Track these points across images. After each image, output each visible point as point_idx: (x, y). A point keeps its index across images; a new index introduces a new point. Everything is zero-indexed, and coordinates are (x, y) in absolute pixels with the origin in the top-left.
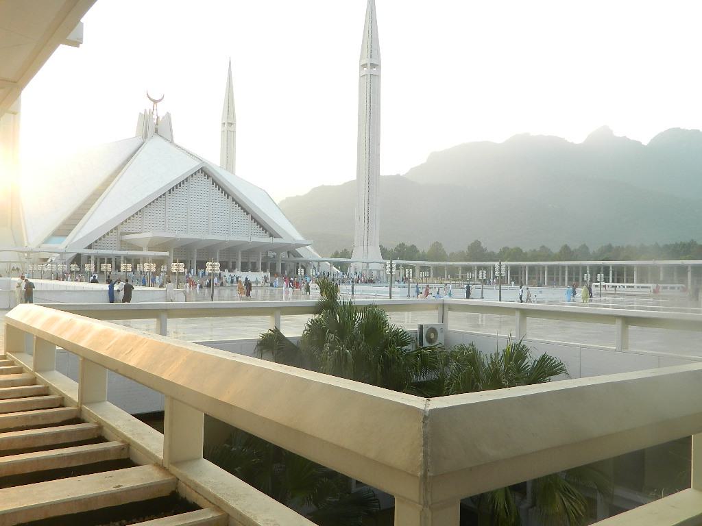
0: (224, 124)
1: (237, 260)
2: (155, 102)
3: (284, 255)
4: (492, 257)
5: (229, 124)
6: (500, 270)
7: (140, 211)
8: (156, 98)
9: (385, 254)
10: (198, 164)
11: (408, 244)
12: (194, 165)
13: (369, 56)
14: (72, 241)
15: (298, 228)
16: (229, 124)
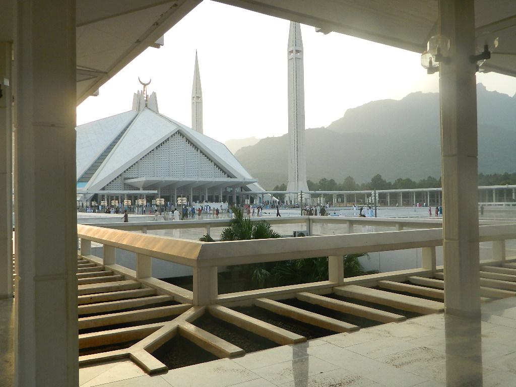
0: (194, 97)
1: (205, 194)
2: (145, 85)
3: (238, 190)
4: (389, 186)
5: (197, 98)
6: (375, 196)
7: (137, 162)
8: (145, 81)
9: (311, 186)
10: (176, 127)
11: (329, 179)
12: (173, 129)
13: (294, 45)
14: (91, 185)
15: (248, 170)
16: (197, 98)
